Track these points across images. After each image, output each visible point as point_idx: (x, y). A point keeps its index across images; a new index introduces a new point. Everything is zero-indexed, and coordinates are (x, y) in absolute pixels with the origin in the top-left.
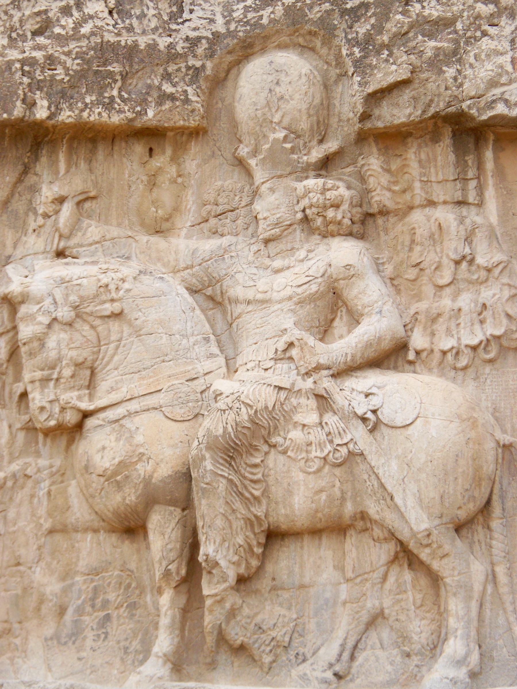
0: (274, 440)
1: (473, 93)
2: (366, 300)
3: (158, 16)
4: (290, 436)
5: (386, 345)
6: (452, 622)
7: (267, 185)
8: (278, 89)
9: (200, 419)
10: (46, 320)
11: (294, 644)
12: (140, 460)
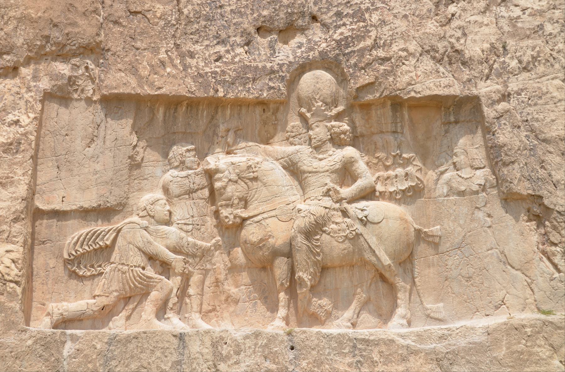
0: (324, 229)
1: (401, 88)
2: (359, 171)
3: (266, 54)
4: (331, 227)
5: (368, 190)
6: (399, 301)
7: (315, 124)
8: (317, 85)
9: (293, 221)
10: (226, 180)
11: (334, 312)
12: (269, 238)
